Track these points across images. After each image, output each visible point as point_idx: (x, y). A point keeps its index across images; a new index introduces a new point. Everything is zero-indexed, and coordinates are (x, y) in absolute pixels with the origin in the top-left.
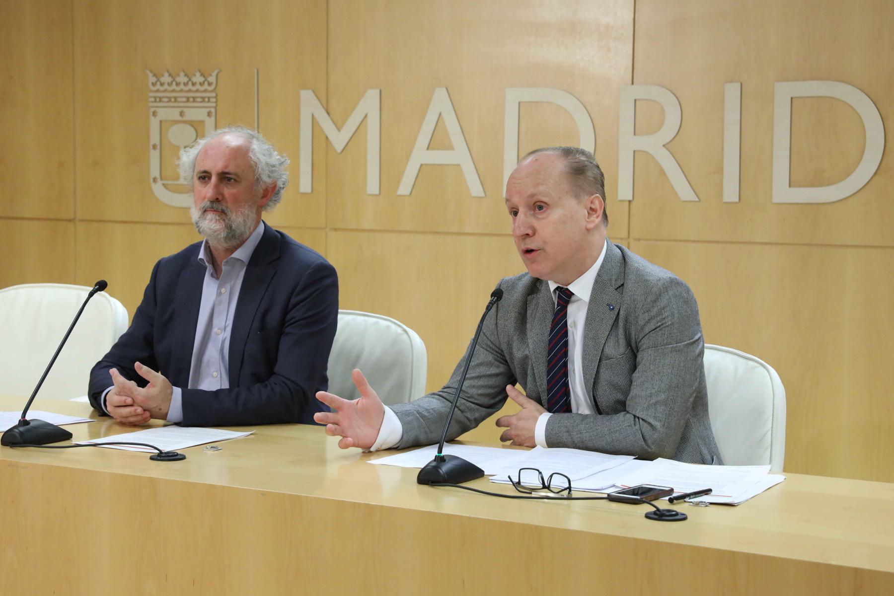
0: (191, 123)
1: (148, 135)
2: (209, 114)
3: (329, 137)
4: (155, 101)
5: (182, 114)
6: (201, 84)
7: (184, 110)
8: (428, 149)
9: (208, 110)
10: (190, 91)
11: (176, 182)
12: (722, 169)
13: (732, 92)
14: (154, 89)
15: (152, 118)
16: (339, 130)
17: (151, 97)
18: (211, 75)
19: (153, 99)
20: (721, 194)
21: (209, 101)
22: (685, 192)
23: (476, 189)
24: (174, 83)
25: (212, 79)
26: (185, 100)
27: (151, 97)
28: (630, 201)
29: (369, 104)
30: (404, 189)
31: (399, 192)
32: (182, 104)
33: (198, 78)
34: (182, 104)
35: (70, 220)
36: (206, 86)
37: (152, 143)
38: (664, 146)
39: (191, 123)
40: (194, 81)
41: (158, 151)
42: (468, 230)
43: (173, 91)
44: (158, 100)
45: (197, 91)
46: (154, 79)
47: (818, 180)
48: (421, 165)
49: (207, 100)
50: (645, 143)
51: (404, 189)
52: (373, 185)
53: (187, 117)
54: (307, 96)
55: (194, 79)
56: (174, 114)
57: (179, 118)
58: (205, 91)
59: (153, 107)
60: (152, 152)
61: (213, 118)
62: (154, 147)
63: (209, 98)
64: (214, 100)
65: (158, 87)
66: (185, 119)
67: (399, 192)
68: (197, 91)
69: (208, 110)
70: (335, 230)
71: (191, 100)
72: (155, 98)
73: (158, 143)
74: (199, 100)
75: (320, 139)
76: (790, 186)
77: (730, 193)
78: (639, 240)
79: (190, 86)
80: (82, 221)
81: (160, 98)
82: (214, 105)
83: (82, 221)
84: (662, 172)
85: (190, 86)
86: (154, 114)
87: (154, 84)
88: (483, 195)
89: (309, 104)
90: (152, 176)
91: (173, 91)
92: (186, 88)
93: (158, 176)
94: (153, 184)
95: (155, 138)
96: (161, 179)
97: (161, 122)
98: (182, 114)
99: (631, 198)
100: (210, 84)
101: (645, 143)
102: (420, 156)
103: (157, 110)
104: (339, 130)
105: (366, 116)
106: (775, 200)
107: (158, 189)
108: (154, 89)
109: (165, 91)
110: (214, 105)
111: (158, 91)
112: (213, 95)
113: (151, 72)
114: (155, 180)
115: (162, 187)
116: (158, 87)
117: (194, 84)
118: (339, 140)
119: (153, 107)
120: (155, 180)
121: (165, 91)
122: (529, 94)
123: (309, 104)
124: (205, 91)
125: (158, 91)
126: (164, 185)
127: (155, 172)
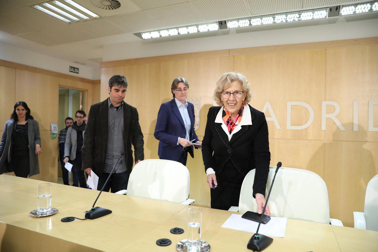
21: (198, 105)
23: (278, 127)
33: (195, 100)
42: (275, 138)
50: (329, 116)
55: (194, 100)
76: (374, 127)
88: (280, 128)
100: (198, 101)
101: (329, 116)
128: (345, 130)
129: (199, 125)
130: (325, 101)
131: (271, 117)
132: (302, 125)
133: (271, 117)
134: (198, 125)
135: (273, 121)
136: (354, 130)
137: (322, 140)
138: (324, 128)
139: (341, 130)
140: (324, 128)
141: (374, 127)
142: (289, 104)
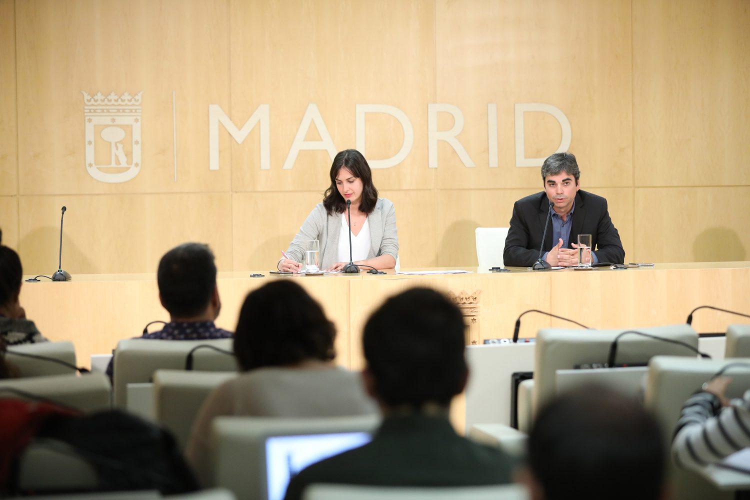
0: (121, 126)
1: (84, 136)
2: (137, 120)
3: (231, 133)
4: (90, 112)
5: (113, 120)
6: (130, 101)
7: (115, 118)
8: (304, 141)
9: (135, 117)
10: (120, 105)
11: (109, 166)
12: (488, 150)
13: (492, 109)
14: (90, 103)
15: (87, 124)
16: (240, 129)
17: (88, 109)
18: (136, 94)
19: (88, 111)
20: (489, 164)
21: (136, 112)
22: (468, 161)
24: (106, 100)
25: (138, 97)
26: (116, 111)
27: (86, 109)
28: (436, 168)
29: (262, 114)
30: (289, 164)
31: (284, 168)
32: (111, 114)
33: (126, 97)
34: (111, 114)
35: (12, 196)
36: (133, 102)
37: (87, 140)
38: (455, 137)
39: (121, 126)
40: (123, 99)
41: (92, 146)
43: (106, 105)
44: (92, 111)
45: (126, 105)
46: (89, 98)
47: (537, 155)
48: (300, 150)
49: (134, 111)
51: (289, 164)
52: (265, 162)
53: (117, 122)
54: (215, 110)
55: (123, 97)
56: (107, 120)
57: (111, 123)
58: (133, 105)
59: (90, 116)
60: (87, 146)
61: (139, 124)
62: (90, 143)
63: (136, 110)
64: (140, 111)
65: (92, 102)
66: (115, 123)
67: (284, 168)
68: (126, 105)
69: (135, 117)
70: (236, 192)
71: (121, 111)
72: (90, 110)
73: (93, 140)
74: (126, 111)
75: (226, 137)
76: (526, 157)
77: (494, 161)
78: (442, 189)
79: (120, 102)
80: (23, 195)
81: (93, 109)
82: (140, 114)
83: (23, 195)
84: (454, 152)
85: (120, 102)
86: (90, 120)
87: (89, 101)
89: (217, 114)
90: (87, 162)
91: (106, 105)
92: (116, 103)
93: (93, 162)
94: (88, 168)
95: (90, 136)
96: (96, 165)
97: (95, 126)
98: (113, 120)
99: (437, 167)
102: (300, 144)
103: (91, 118)
104: (240, 129)
105: (259, 121)
106: (518, 165)
107: (93, 172)
108: (90, 103)
109: (99, 105)
110: (140, 114)
111: (93, 105)
112: (140, 107)
113: (86, 93)
114: (91, 165)
115: (97, 169)
116: (92, 102)
117: (122, 100)
118: (240, 136)
119: (90, 116)
120: (91, 165)
121: (99, 105)
122: (371, 108)
123: (217, 114)
124: (133, 105)
125: (93, 105)
126: (97, 168)
127: (90, 157)
128: (474, 166)
129: (140, 165)
130: (435, 102)
131: (322, 140)
132: (390, 158)
133: (322, 140)
134: (137, 165)
135: (326, 150)
136: (491, 166)
137: (430, 190)
138: (433, 162)
139: (466, 166)
140: (433, 162)
141: (526, 157)
142: (361, 110)
